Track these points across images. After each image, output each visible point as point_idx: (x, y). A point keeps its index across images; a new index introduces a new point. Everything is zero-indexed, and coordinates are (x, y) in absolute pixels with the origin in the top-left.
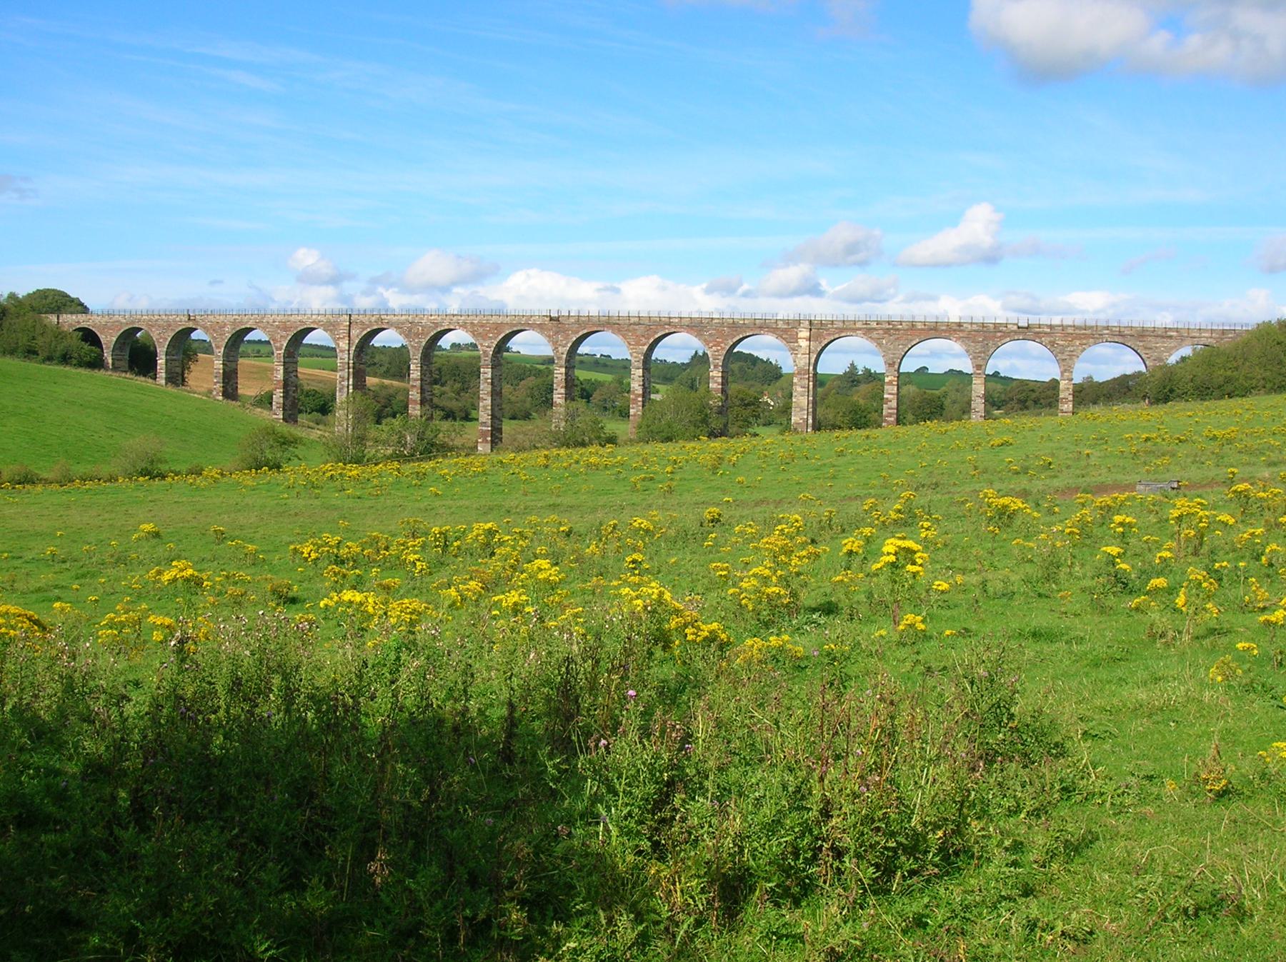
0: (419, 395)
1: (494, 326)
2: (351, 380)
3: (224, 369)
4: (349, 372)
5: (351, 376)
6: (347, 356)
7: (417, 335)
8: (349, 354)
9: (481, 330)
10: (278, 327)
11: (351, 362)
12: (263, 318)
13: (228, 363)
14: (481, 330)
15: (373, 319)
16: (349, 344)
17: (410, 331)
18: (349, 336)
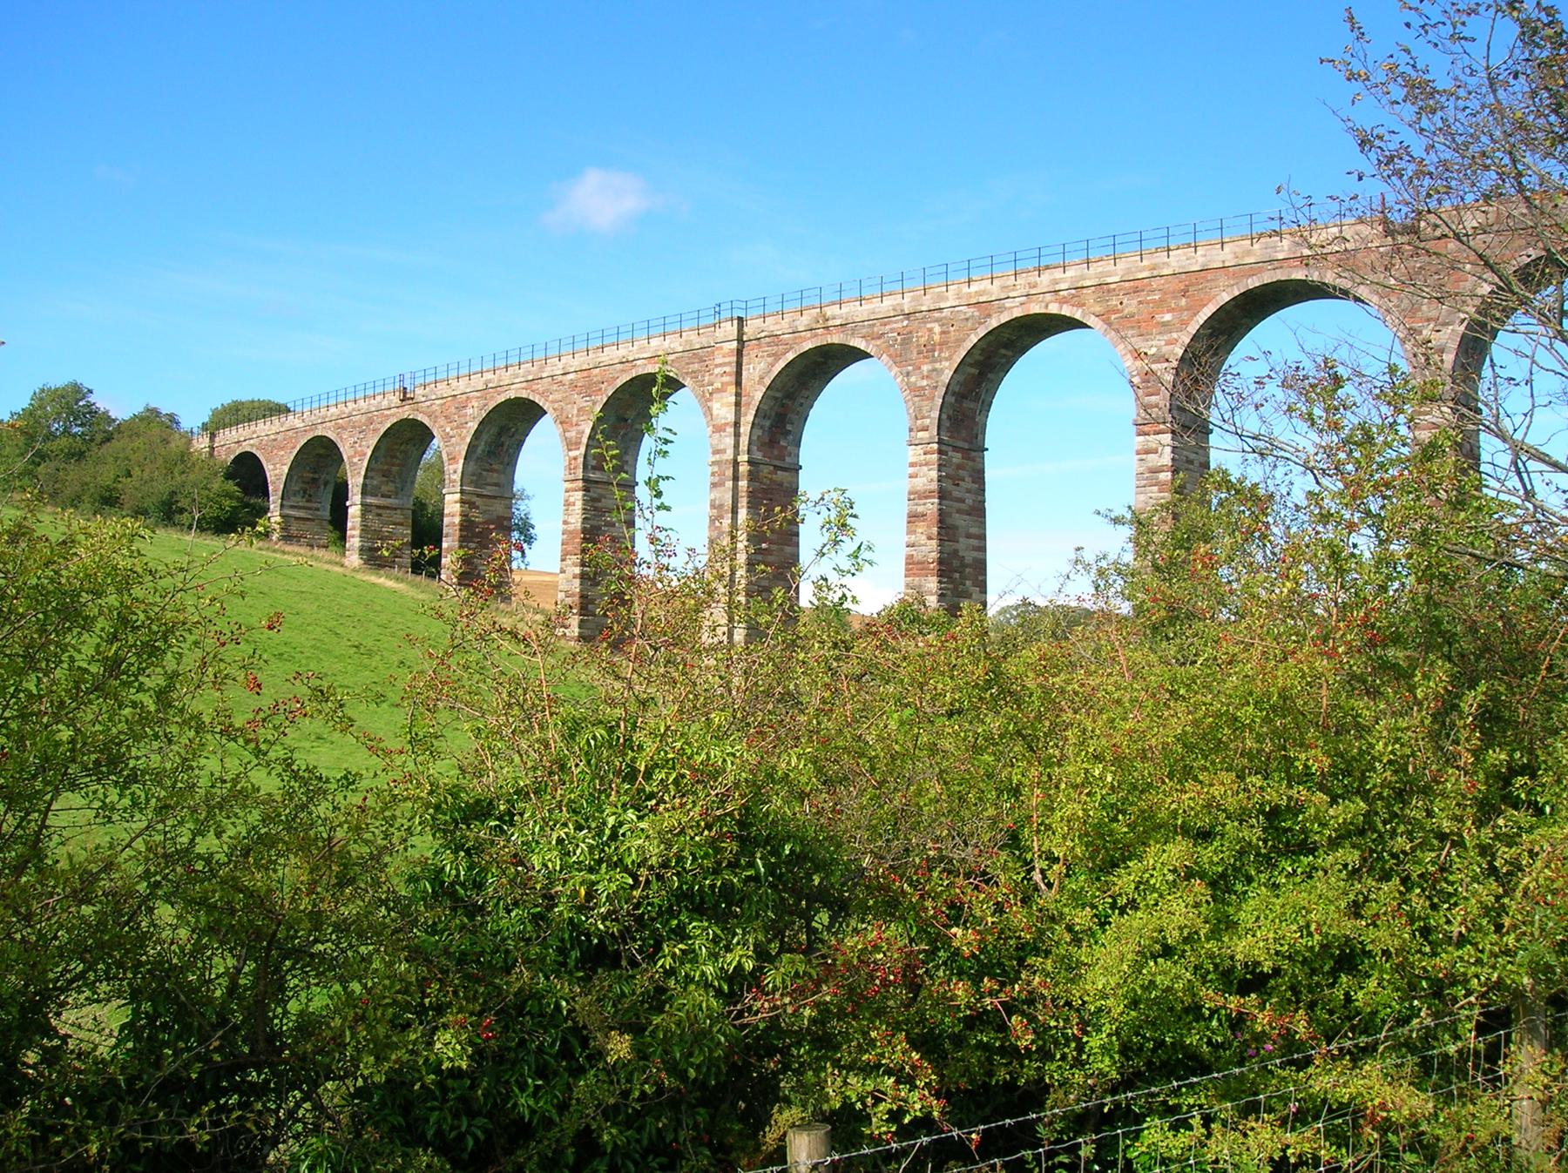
0: (934, 543)
1: (1175, 285)
2: (743, 514)
3: (464, 515)
4: (735, 488)
5: (743, 502)
6: (730, 441)
7: (929, 350)
8: (737, 435)
9: (1131, 305)
10: (573, 386)
11: (743, 458)
12: (541, 369)
13: (478, 501)
14: (1131, 305)
15: (804, 321)
16: (738, 404)
17: (906, 342)
18: (738, 383)
